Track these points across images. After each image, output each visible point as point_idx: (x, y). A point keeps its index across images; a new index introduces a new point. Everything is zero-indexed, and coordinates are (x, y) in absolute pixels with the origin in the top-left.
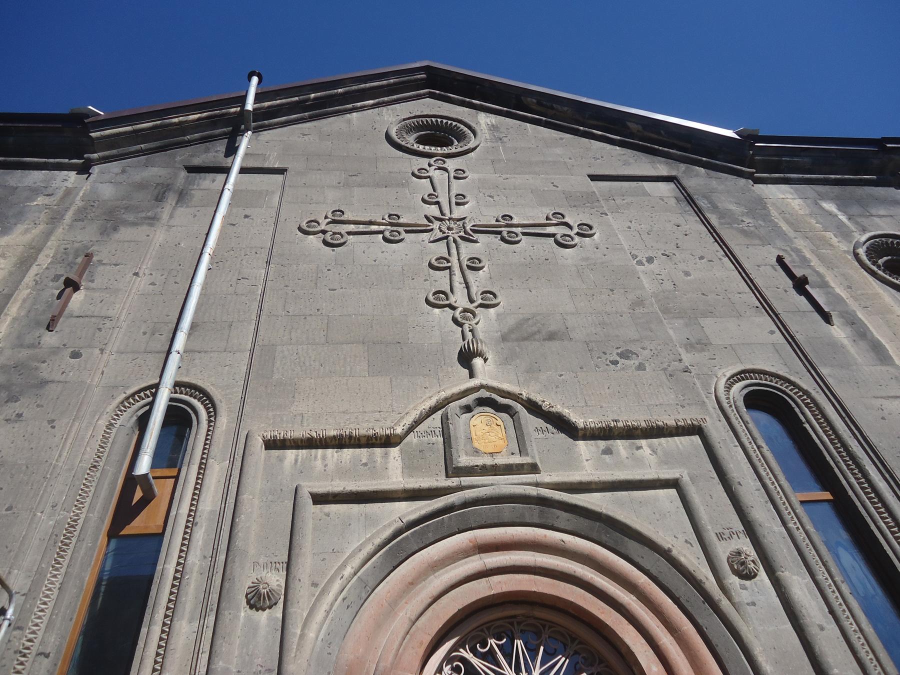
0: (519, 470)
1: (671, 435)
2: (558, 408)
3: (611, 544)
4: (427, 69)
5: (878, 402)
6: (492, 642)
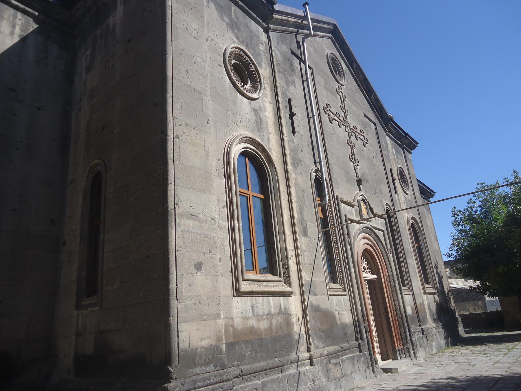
4: (335, 25)
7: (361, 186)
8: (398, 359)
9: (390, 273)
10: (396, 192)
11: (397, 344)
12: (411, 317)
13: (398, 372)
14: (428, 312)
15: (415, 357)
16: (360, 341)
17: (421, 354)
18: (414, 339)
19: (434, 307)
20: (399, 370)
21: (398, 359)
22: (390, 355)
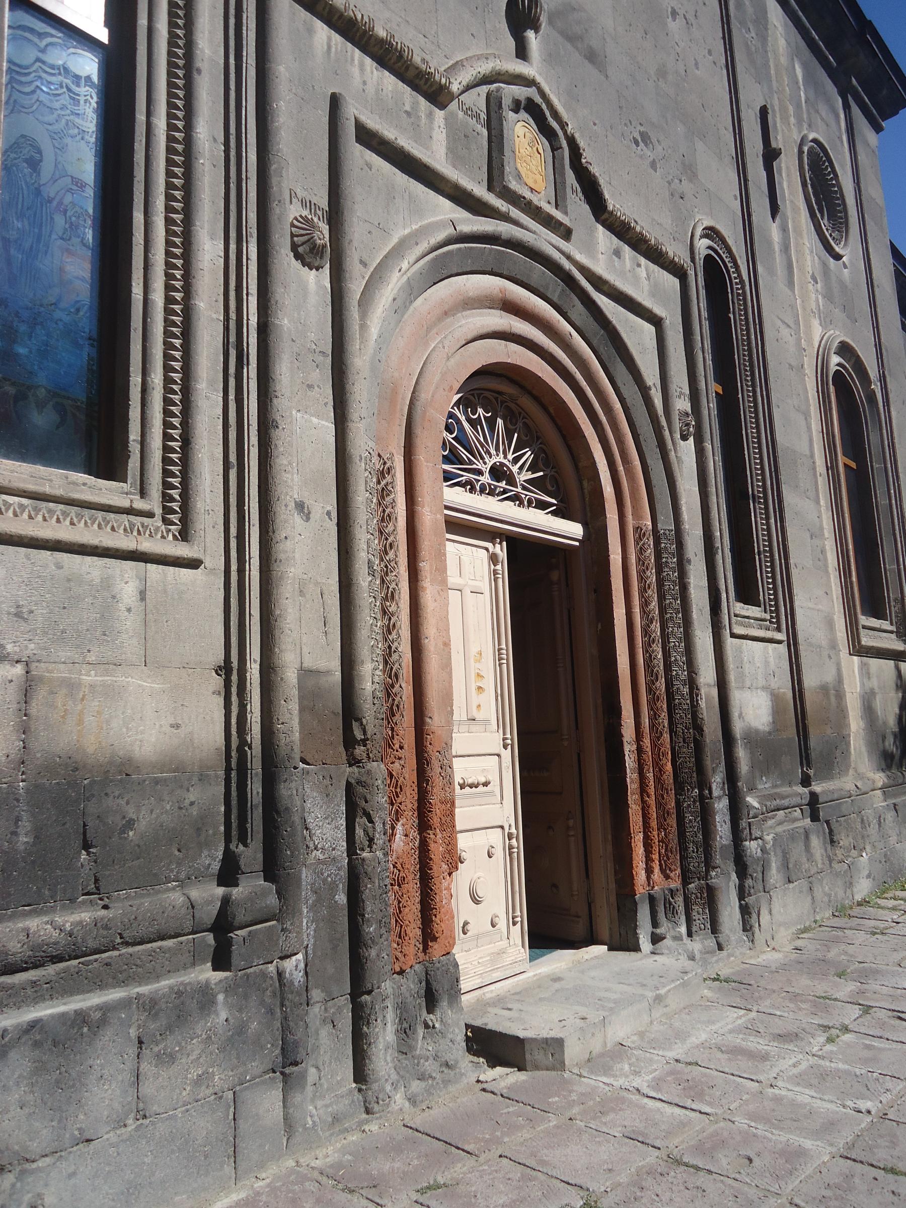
0: (555, 228)
1: (663, 267)
2: (595, 170)
3: (604, 357)
5: (779, 323)
6: (480, 411)
7: (530, 34)
8: (636, 948)
9: (666, 524)
10: (775, 210)
11: (649, 871)
12: (754, 739)
13: (560, 1065)
14: (856, 724)
15: (747, 928)
16: (251, 888)
17: (784, 911)
18: (752, 847)
19: (889, 709)
20: (573, 1052)
21: (636, 948)
22: (604, 926)
